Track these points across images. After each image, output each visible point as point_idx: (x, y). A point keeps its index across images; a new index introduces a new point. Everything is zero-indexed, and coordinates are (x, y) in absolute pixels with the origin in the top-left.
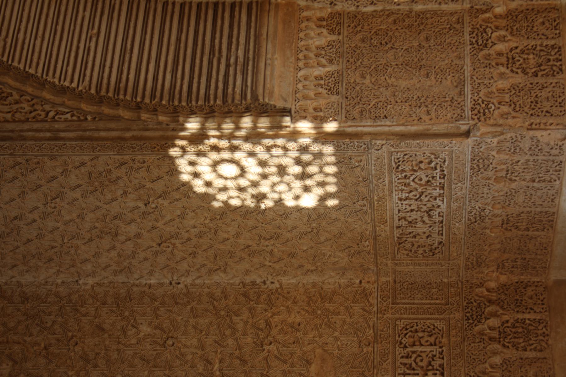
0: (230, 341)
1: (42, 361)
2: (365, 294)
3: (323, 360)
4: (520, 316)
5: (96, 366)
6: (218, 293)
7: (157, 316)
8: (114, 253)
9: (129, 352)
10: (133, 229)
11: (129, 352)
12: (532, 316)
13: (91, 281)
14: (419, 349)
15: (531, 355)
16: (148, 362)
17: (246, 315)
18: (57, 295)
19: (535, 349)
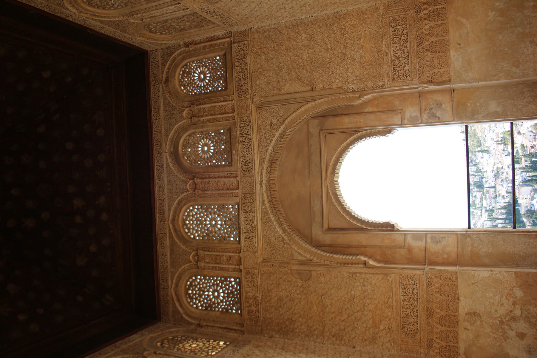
0: (333, 35)
1: (274, 53)
2: (378, 9)
3: (365, 37)
4: (436, 7)
5: (290, 51)
6: (326, 18)
7: (307, 30)
8: (287, 13)
9: (300, 45)
10: (290, 6)
11: (300, 45)
12: (440, 7)
13: (284, 21)
14: (398, 27)
15: (440, 22)
16: (306, 47)
17: (336, 24)
18: (274, 28)
19: (441, 20)
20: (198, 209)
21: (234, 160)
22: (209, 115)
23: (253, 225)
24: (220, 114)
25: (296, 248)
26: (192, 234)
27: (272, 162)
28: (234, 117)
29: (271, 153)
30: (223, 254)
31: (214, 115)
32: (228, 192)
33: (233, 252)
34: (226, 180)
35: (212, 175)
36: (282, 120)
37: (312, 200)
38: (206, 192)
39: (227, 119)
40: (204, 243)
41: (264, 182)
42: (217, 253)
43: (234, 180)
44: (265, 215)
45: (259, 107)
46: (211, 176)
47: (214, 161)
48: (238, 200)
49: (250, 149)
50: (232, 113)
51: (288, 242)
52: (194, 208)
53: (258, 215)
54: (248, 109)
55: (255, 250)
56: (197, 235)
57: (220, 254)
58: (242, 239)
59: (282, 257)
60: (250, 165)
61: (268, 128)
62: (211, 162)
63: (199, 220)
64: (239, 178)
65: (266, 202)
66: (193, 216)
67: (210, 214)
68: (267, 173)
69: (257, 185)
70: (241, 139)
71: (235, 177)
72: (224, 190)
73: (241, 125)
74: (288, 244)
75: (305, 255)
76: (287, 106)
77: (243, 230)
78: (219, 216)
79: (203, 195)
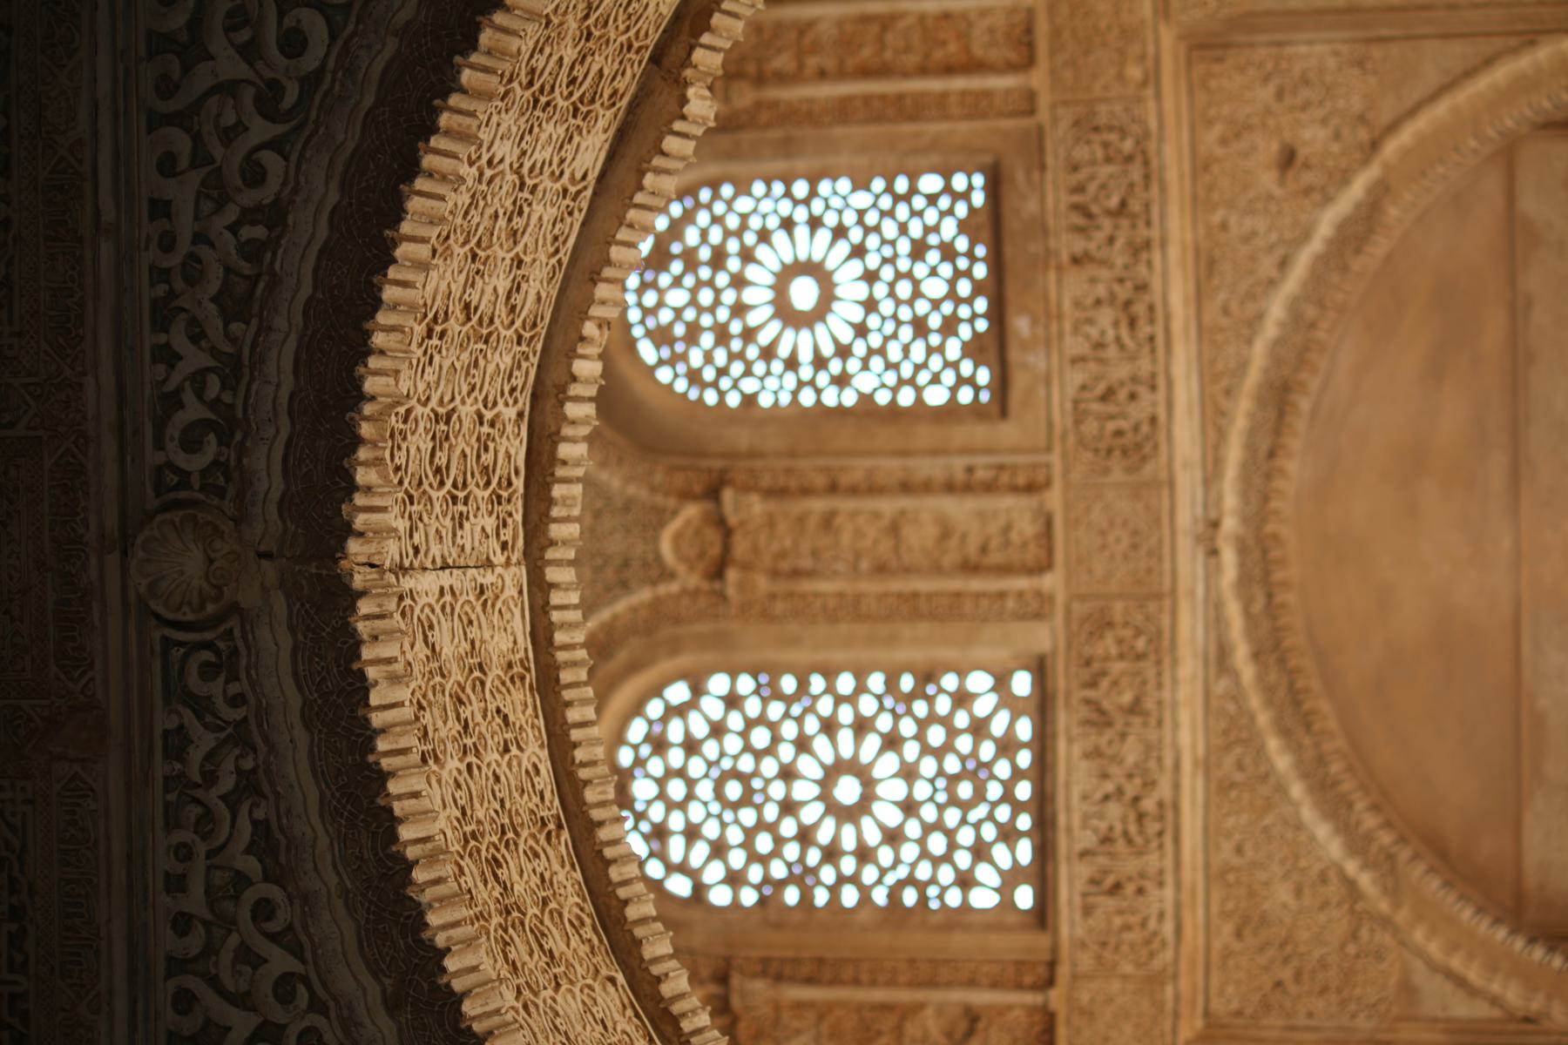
20: (732, 701)
21: (1019, 381)
22: (842, 75)
23: (1148, 804)
24: (923, 71)
25: (1434, 949)
26: (683, 868)
27: (1279, 397)
28: (1031, 96)
29: (1278, 342)
30: (919, 995)
31: (884, 71)
32: (976, 584)
33: (995, 985)
34: (959, 509)
35: (857, 469)
36: (1363, 135)
37: (1526, 648)
38: (807, 586)
39: (978, 106)
40: (778, 926)
41: (1230, 524)
42: (880, 995)
43: (1017, 511)
44: (1230, 731)
45: (1206, 46)
46: (845, 480)
47: (864, 382)
48: (1041, 637)
49: (1140, 309)
50: (1011, 68)
51: (1384, 906)
52: (698, 691)
53: (1185, 737)
54: (1134, 49)
55: (1157, 963)
57: (903, 996)
58: (1067, 893)
59: (1343, 1003)
60: (1139, 411)
61: (1267, 179)
62: (842, 381)
63: (735, 774)
64: (1054, 499)
65: (1241, 653)
66: (691, 746)
67: (829, 727)
68: (1245, 479)
69: (1185, 544)
70: (1079, 245)
71: (1031, 488)
72: (937, 570)
73: (1081, 153)
74: (1386, 922)
75: (1496, 987)
76: (1395, 49)
77: (1074, 835)
79: (779, 607)
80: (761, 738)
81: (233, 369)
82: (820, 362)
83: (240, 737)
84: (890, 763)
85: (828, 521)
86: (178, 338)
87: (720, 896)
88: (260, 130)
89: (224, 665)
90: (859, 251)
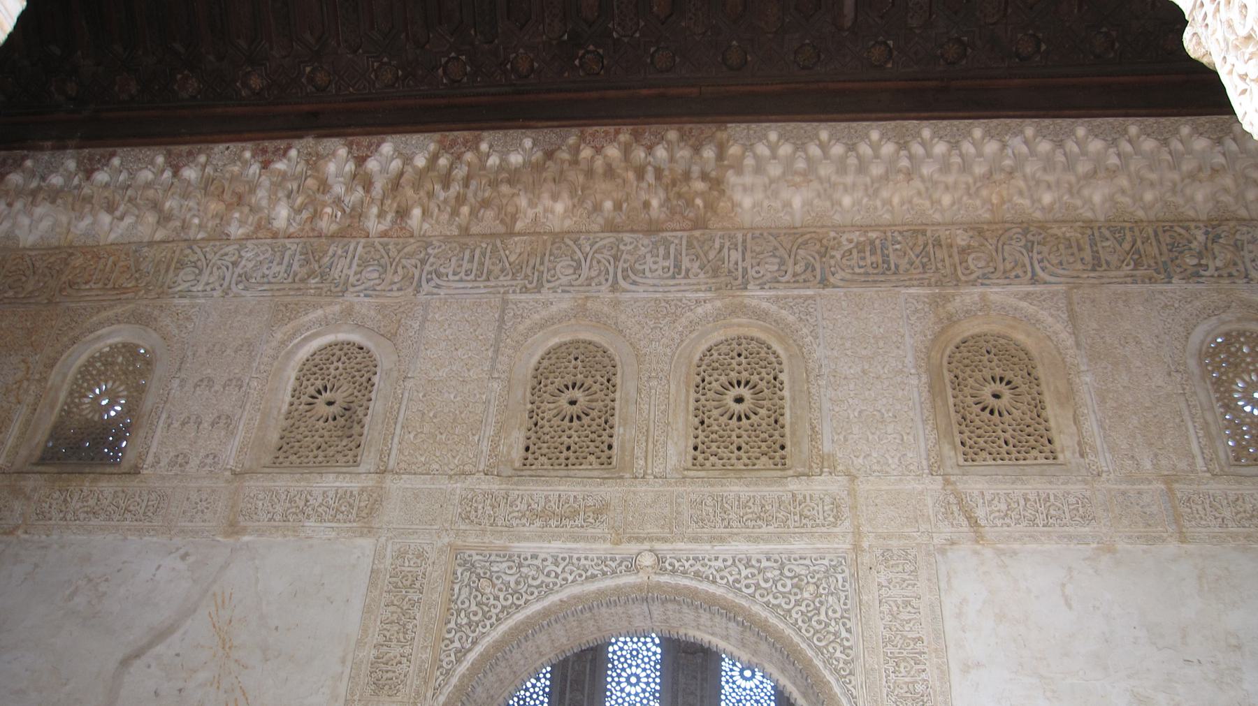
20: (655, 654)
47: (726, 687)
52: (657, 645)
56: (616, 648)
67: (648, 676)
78: (644, 691)
80: (646, 660)
81: (684, 573)
82: (731, 677)
83: (614, 572)
84: (639, 690)
85: (695, 678)
86: (691, 562)
87: (611, 649)
88: (731, 579)
89: (628, 569)
90: (757, 687)
